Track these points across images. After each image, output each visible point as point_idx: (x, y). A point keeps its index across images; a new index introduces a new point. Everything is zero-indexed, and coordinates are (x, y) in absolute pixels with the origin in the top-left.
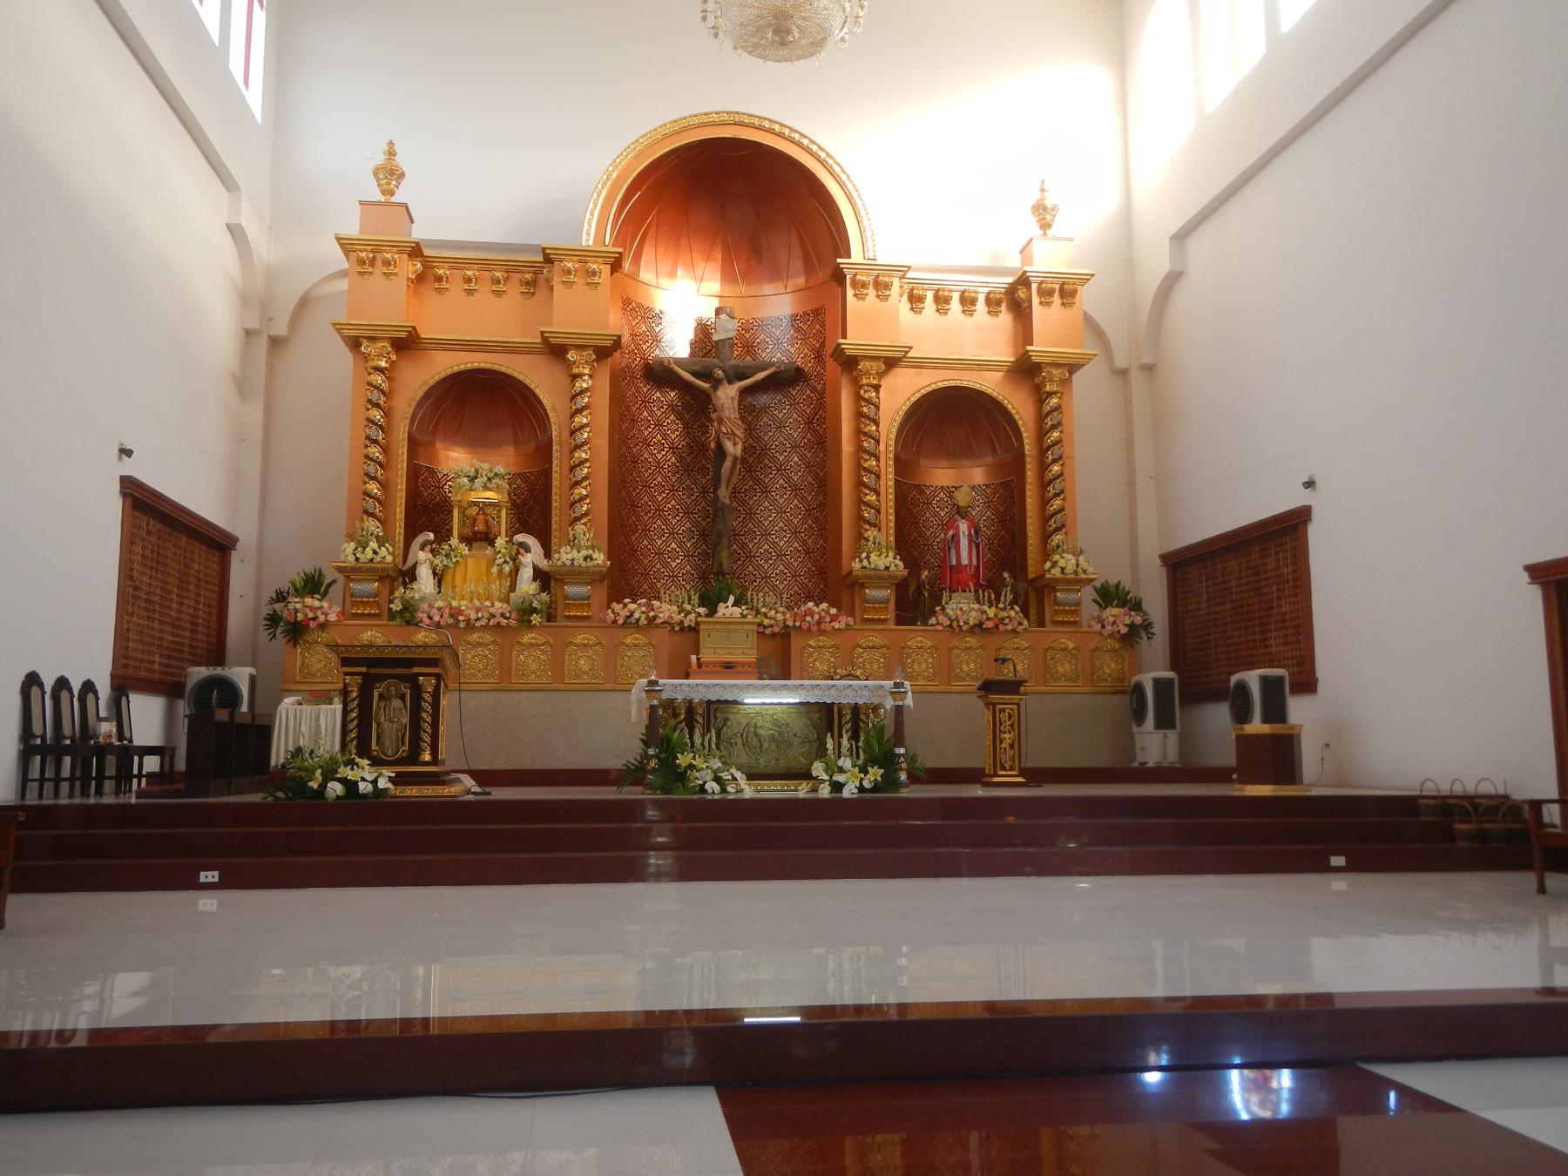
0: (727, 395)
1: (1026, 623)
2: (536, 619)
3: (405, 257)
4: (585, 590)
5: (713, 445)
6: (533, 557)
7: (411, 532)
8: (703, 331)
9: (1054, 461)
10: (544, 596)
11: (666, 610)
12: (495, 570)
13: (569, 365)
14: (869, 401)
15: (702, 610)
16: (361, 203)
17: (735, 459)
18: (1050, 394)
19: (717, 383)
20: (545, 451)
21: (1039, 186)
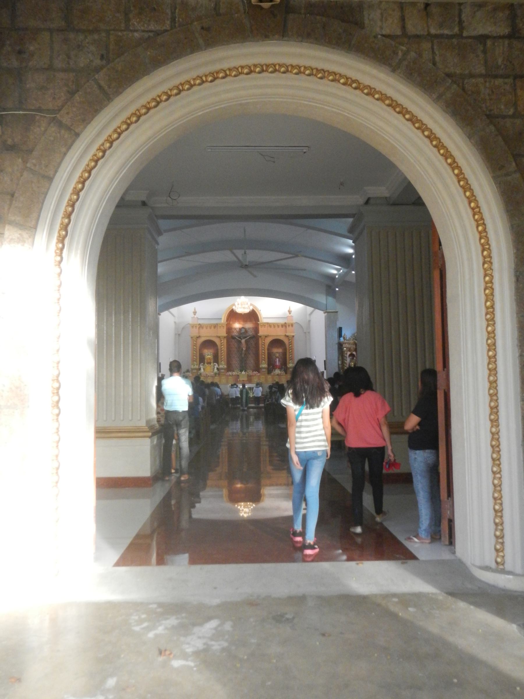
0: (243, 341)
1: (285, 374)
2: (217, 375)
3: (198, 325)
4: (223, 371)
5: (241, 348)
6: (216, 366)
7: (200, 364)
8: (240, 329)
9: (290, 350)
10: (218, 372)
11: (234, 373)
12: (211, 368)
13: (221, 339)
14: (263, 342)
15: (240, 372)
16: (192, 317)
17: (244, 351)
18: (290, 340)
19: (242, 339)
20: (217, 350)
21: (289, 307)
